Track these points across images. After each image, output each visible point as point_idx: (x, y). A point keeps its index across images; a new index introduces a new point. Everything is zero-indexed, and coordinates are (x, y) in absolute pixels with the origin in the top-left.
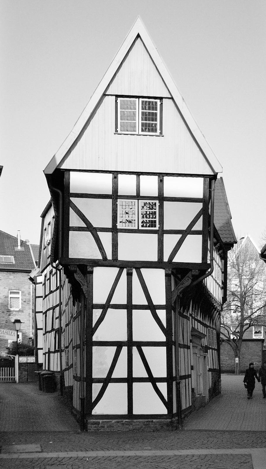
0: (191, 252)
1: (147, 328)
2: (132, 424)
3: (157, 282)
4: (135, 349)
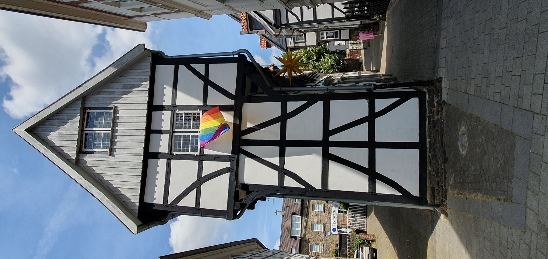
0: (226, 76)
1: (307, 123)
2: (434, 144)
3: (257, 112)
4: (332, 138)
